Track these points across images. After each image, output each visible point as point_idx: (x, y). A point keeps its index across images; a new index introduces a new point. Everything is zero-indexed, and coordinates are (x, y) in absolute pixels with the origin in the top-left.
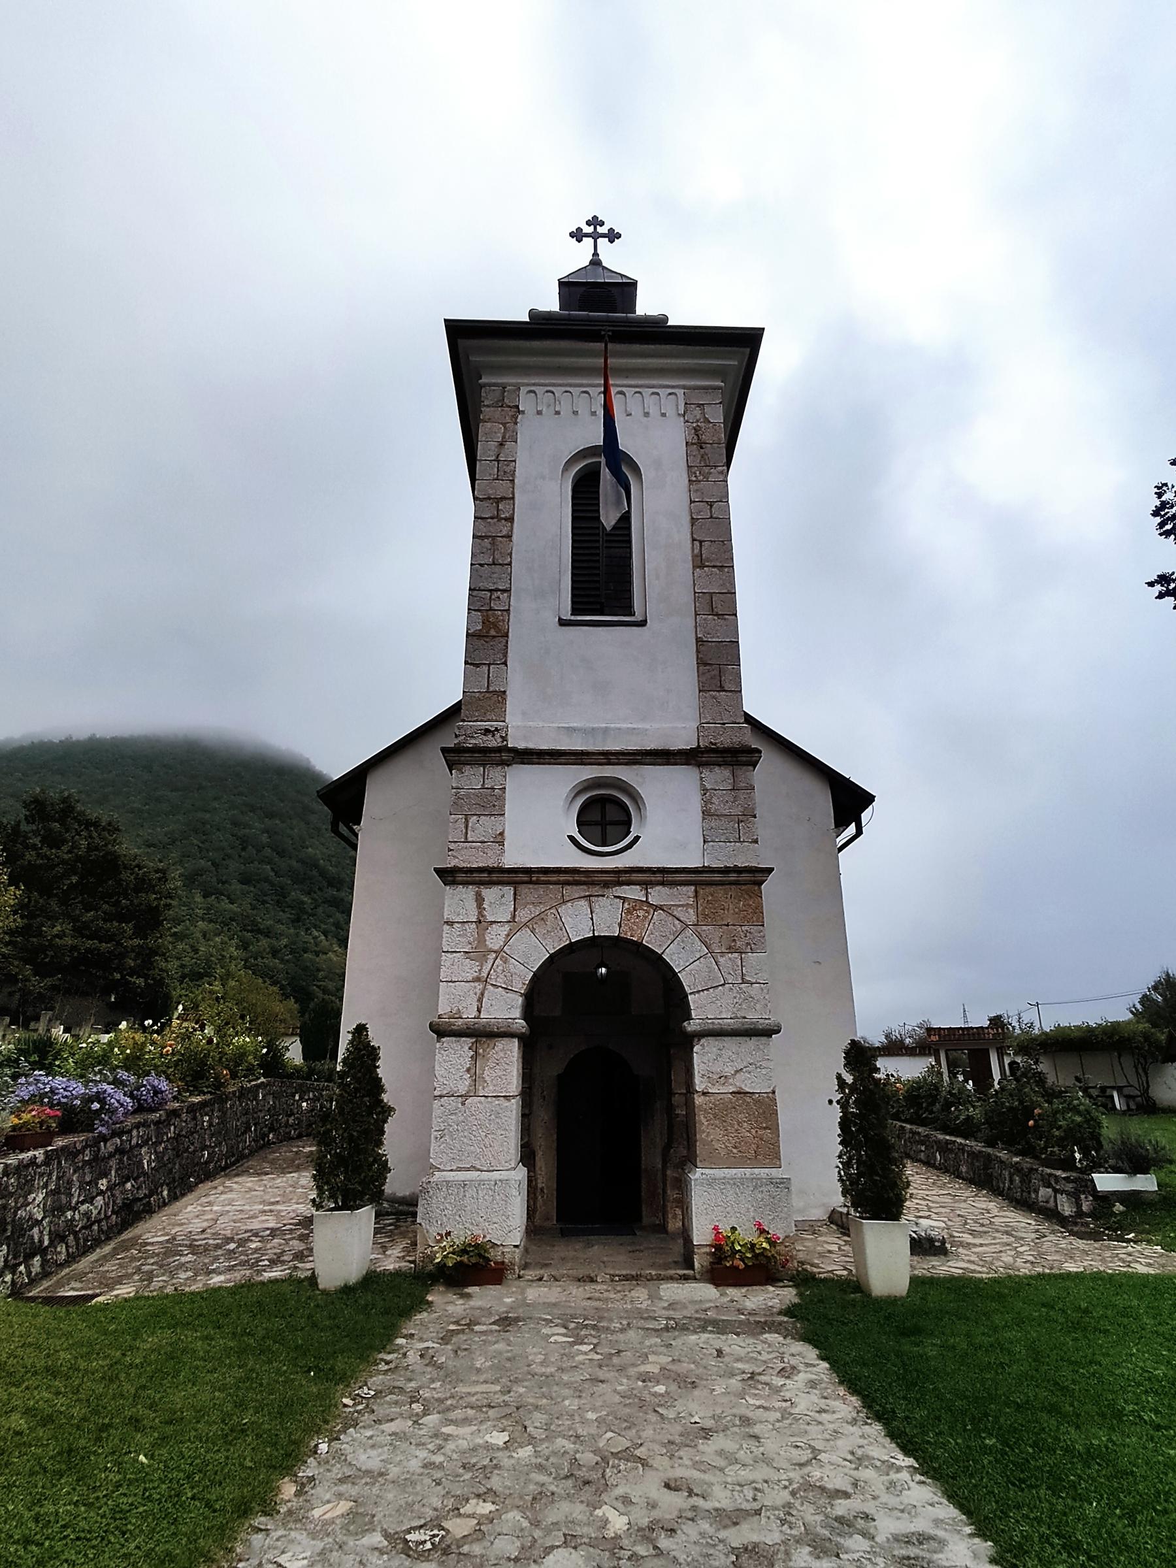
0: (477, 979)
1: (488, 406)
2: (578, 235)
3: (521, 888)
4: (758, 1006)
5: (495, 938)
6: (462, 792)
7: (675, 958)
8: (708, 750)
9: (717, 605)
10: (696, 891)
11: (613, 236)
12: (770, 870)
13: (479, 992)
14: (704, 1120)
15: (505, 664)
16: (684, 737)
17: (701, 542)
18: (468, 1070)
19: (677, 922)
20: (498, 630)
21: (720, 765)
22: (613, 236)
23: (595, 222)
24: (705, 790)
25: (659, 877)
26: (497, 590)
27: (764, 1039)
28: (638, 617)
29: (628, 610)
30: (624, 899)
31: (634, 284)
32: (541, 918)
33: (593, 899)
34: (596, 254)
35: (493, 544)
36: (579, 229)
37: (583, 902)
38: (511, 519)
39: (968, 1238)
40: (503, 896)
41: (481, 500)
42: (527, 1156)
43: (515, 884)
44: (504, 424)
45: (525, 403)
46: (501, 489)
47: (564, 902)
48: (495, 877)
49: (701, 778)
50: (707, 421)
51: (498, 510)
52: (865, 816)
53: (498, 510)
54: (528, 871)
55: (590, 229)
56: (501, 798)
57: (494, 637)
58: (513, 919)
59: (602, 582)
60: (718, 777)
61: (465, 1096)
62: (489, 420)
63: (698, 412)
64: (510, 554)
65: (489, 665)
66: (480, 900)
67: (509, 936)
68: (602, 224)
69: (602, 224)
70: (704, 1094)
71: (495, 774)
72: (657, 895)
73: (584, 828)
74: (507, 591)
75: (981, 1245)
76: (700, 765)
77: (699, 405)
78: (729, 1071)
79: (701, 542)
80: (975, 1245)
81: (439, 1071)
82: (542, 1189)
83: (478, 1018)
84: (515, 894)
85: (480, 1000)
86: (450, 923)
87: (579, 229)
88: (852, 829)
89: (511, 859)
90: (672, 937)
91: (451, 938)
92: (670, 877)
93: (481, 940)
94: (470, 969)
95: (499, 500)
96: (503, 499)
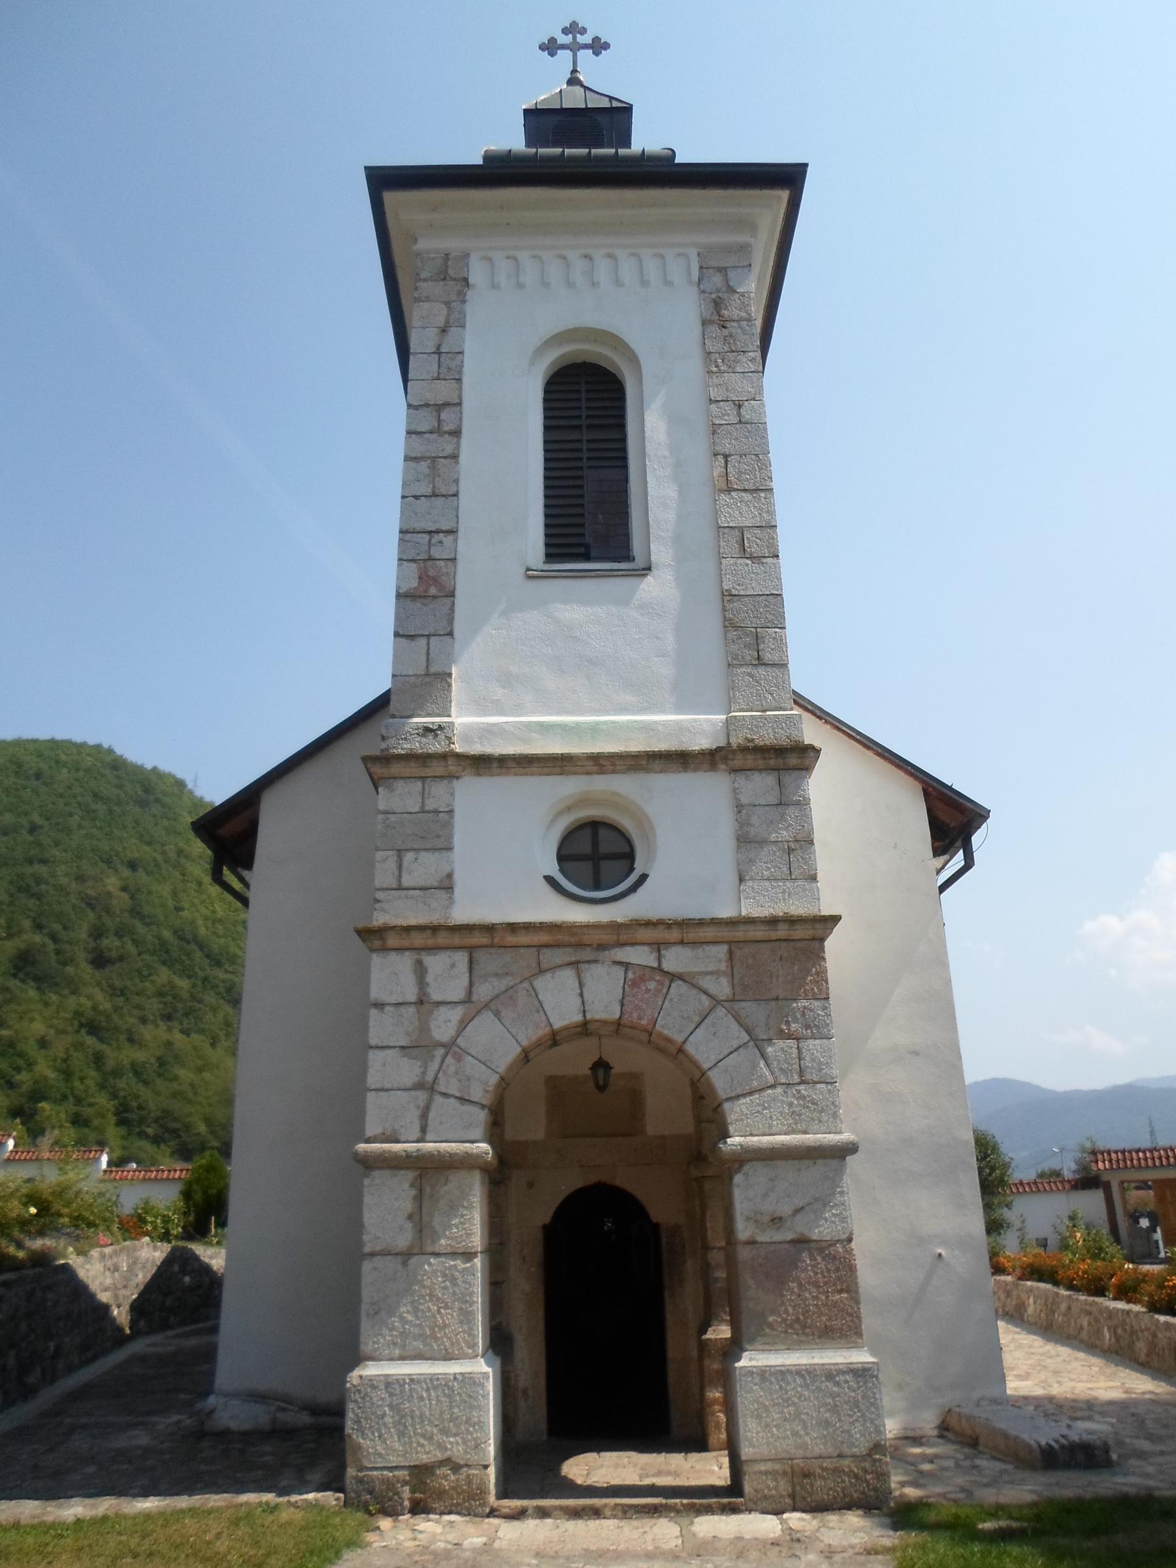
0: (419, 1086)
1: (425, 280)
3: (480, 955)
4: (824, 1117)
5: (443, 1025)
6: (393, 818)
8: (743, 749)
9: (754, 545)
10: (731, 953)
12: (835, 919)
13: (422, 1105)
14: (751, 1282)
15: (451, 634)
17: (726, 457)
18: (410, 1217)
19: (704, 997)
20: (441, 587)
21: (760, 770)
24: (739, 807)
25: (675, 934)
26: (438, 532)
27: (834, 1163)
28: (639, 562)
29: (627, 557)
30: (626, 966)
31: (627, 110)
32: (506, 996)
33: (583, 966)
34: (574, 71)
35: (433, 468)
37: (568, 975)
38: (457, 433)
39: (1145, 1445)
40: (453, 965)
41: (417, 408)
42: (500, 1342)
43: (471, 949)
44: (447, 304)
45: (477, 273)
46: (442, 391)
47: (541, 971)
48: (442, 939)
49: (735, 790)
51: (439, 421)
52: (976, 839)
53: (439, 421)
54: (489, 929)
56: (448, 826)
57: (434, 597)
58: (468, 1000)
59: (588, 520)
60: (759, 786)
61: (406, 1255)
62: (428, 299)
63: (717, 280)
64: (457, 481)
65: (428, 636)
66: (420, 970)
67: (463, 1025)
70: (752, 1242)
71: (438, 790)
72: (676, 959)
73: (570, 865)
74: (452, 532)
75: (1162, 1453)
76: (735, 771)
77: (722, 270)
78: (785, 1209)
79: (726, 457)
80: (1154, 1454)
81: (369, 1218)
82: (525, 1391)
83: (421, 1140)
84: (471, 962)
85: (424, 1116)
86: (380, 1006)
88: (958, 860)
90: (697, 1019)
91: (381, 1028)
92: (692, 935)
93: (424, 1029)
94: (408, 1071)
96: (447, 405)
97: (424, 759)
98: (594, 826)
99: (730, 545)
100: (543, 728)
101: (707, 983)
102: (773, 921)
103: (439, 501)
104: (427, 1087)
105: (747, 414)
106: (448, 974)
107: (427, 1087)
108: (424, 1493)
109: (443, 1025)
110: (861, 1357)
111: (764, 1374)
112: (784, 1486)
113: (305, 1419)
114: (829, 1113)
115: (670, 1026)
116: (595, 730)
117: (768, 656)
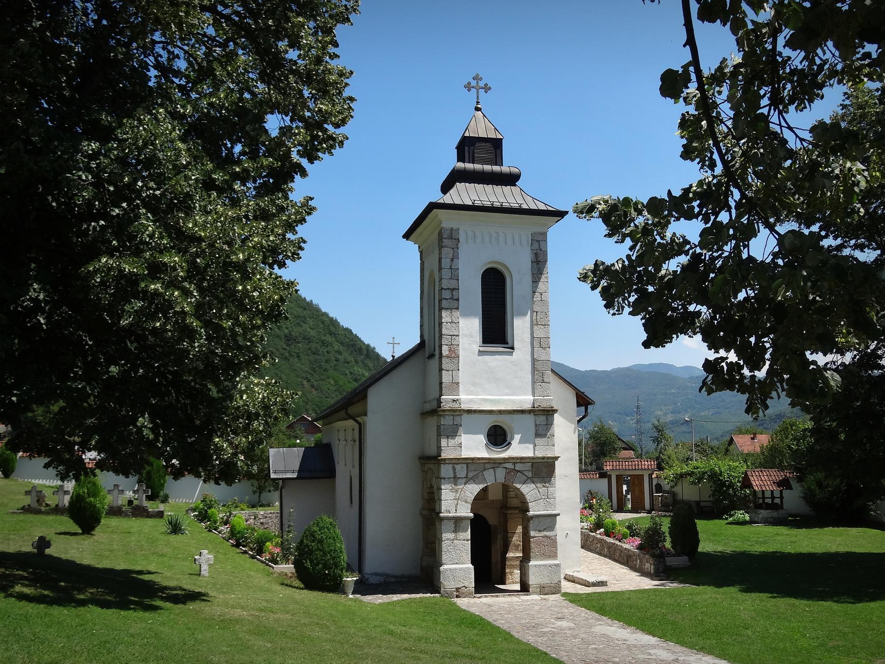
11: (487, 88)
22: (487, 88)
23: (477, 78)
24: (536, 425)
28: (510, 345)
34: (478, 103)
36: (469, 83)
37: (492, 470)
38: (458, 300)
50: (541, 250)
54: (473, 459)
55: (474, 83)
58: (466, 477)
60: (542, 419)
62: (446, 247)
63: (536, 245)
68: (481, 79)
69: (481, 79)
71: (457, 418)
74: (458, 336)
86: (444, 478)
87: (469, 83)
89: (466, 454)
96: (454, 289)
97: (454, 411)
98: (495, 426)
100: (485, 400)
101: (525, 473)
102: (543, 458)
103: (454, 325)
105: (543, 298)
108: (459, 593)
110: (556, 562)
111: (535, 566)
112: (538, 590)
113: (393, 580)
114: (553, 505)
116: (499, 401)
117: (546, 380)
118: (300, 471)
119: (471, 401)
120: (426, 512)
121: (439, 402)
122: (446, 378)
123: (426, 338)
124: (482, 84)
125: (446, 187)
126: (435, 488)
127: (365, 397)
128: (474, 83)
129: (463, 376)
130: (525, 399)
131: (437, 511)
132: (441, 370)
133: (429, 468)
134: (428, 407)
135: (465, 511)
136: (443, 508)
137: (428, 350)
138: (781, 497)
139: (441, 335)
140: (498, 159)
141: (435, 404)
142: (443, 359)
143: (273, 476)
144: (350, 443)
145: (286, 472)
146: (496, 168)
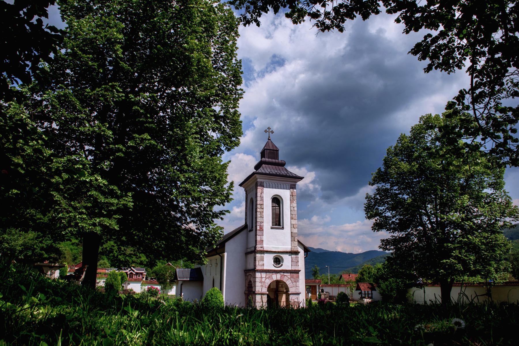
2: (266, 131)
5: (263, 280)
7: (288, 283)
12: (300, 271)
16: (289, 250)
23: (269, 128)
29: (279, 225)
55: (268, 130)
71: (262, 255)
89: (265, 268)
95: (261, 205)
99: (292, 227)
100: (273, 247)
104: (262, 286)
106: (264, 275)
107: (262, 286)
109: (263, 280)
115: (284, 281)
118: (190, 278)
119: (267, 247)
120: (247, 292)
121: (255, 247)
122: (258, 238)
123: (248, 223)
124: (270, 130)
125: (257, 167)
126: (253, 282)
127: (224, 246)
128: (268, 130)
129: (265, 238)
130: (288, 248)
131: (253, 290)
132: (256, 235)
133: (249, 273)
134: (249, 250)
135: (265, 290)
136: (257, 290)
137: (249, 227)
138: (372, 294)
139: (256, 222)
140: (277, 157)
141: (253, 249)
142: (258, 231)
143: (179, 279)
144: (214, 265)
145: (184, 278)
146: (277, 161)
